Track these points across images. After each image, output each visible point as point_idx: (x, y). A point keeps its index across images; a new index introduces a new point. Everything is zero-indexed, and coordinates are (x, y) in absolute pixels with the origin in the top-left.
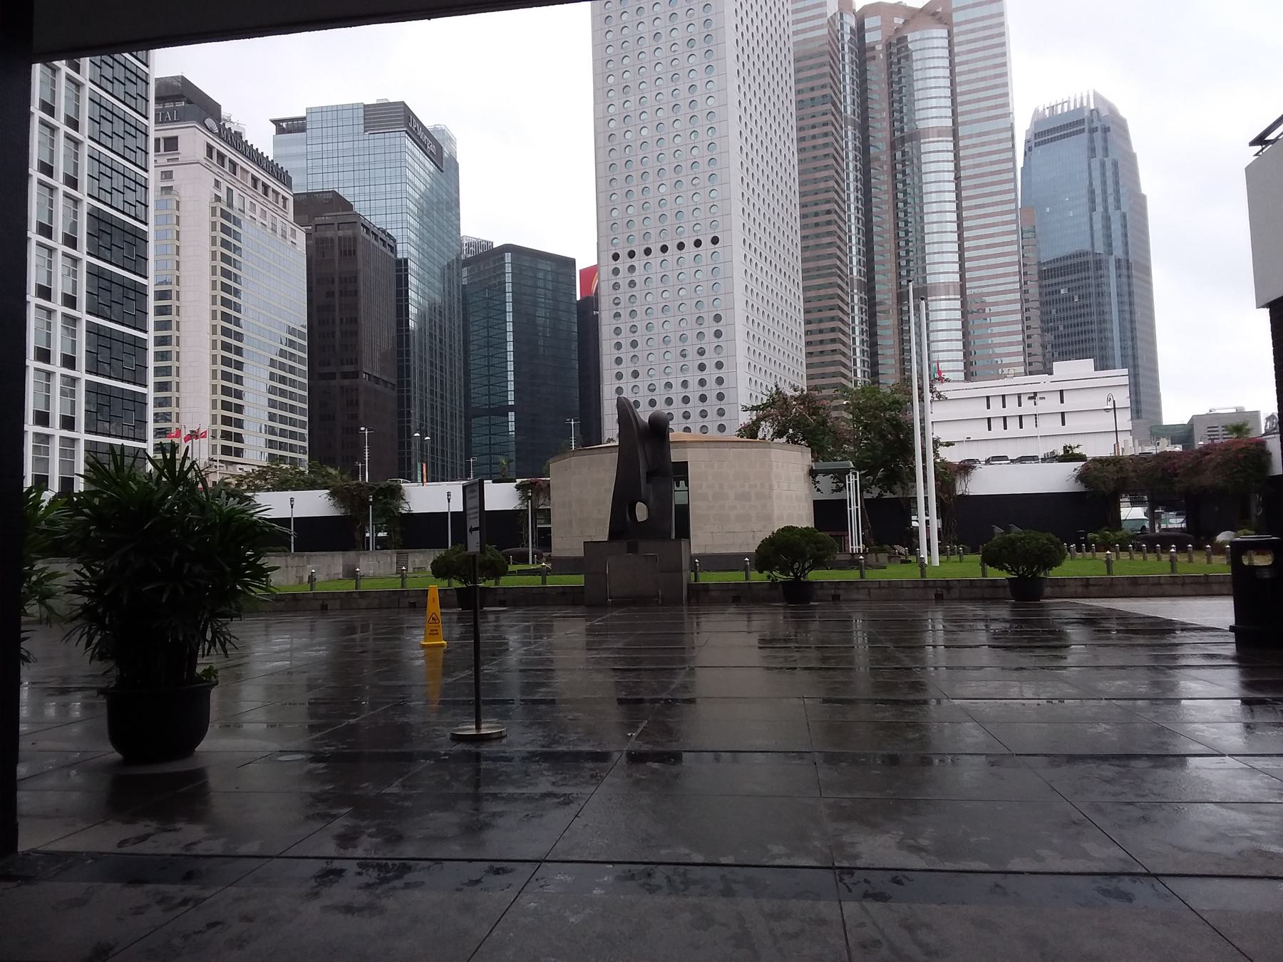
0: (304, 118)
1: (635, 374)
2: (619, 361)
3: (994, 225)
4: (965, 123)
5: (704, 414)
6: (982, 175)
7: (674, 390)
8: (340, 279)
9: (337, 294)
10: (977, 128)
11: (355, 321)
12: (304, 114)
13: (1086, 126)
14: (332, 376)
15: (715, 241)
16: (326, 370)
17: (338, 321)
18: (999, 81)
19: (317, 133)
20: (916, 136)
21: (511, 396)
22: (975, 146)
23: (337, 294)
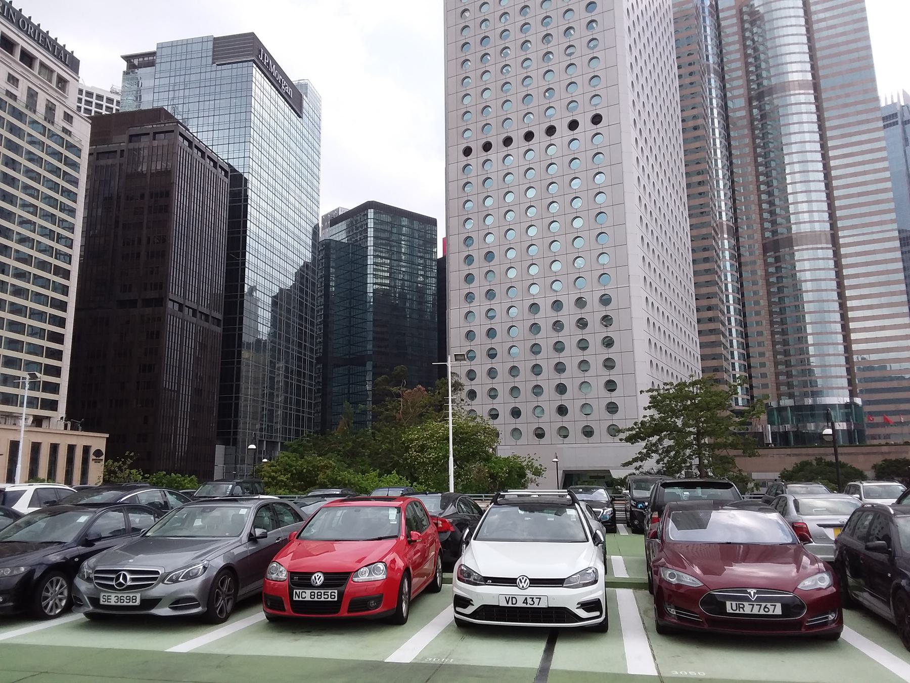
0: (153, 54)
1: (490, 294)
2: (469, 278)
3: (865, 173)
4: (826, 77)
5: (583, 345)
6: (849, 125)
7: (541, 314)
8: (151, 195)
11: (164, 240)
12: (153, 49)
13: (899, 119)
14: (133, 303)
15: (597, 119)
17: (144, 240)
18: (858, 35)
19: (165, 67)
22: (838, 97)
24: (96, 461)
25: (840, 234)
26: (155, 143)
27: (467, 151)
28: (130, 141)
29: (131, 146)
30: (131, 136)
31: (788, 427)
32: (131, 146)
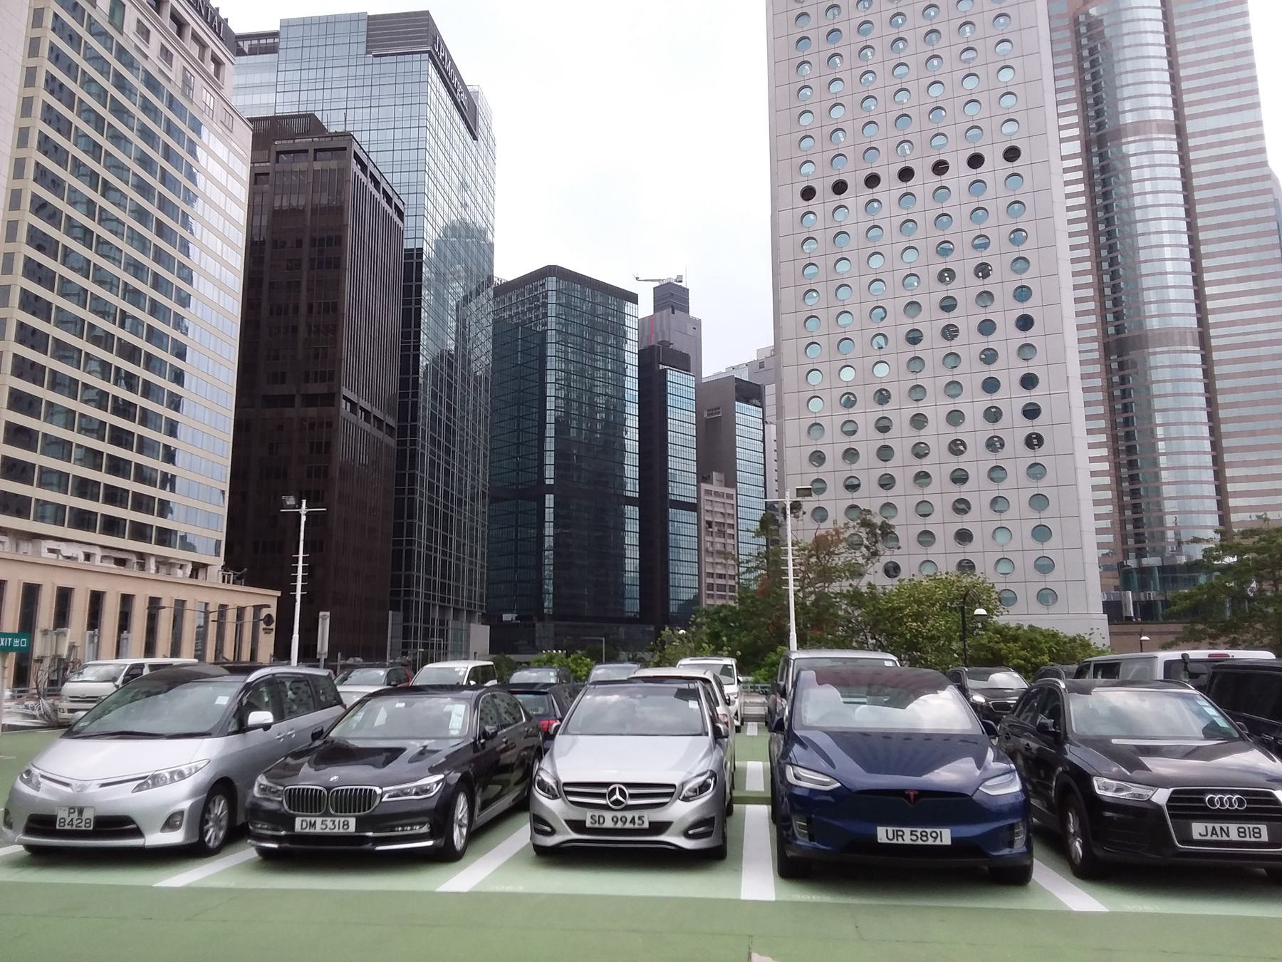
0: (275, 35)
8: (313, 241)
9: (305, 265)
10: (1211, 123)
11: (333, 308)
14: (288, 401)
16: (279, 390)
17: (303, 309)
19: (293, 54)
20: (1119, 133)
21: (550, 473)
22: (1210, 146)
23: (305, 265)
24: (267, 631)
25: (1212, 332)
26: (318, 166)
27: (808, 193)
28: (277, 161)
29: (278, 167)
30: (278, 153)
31: (1153, 595)
32: (278, 167)
